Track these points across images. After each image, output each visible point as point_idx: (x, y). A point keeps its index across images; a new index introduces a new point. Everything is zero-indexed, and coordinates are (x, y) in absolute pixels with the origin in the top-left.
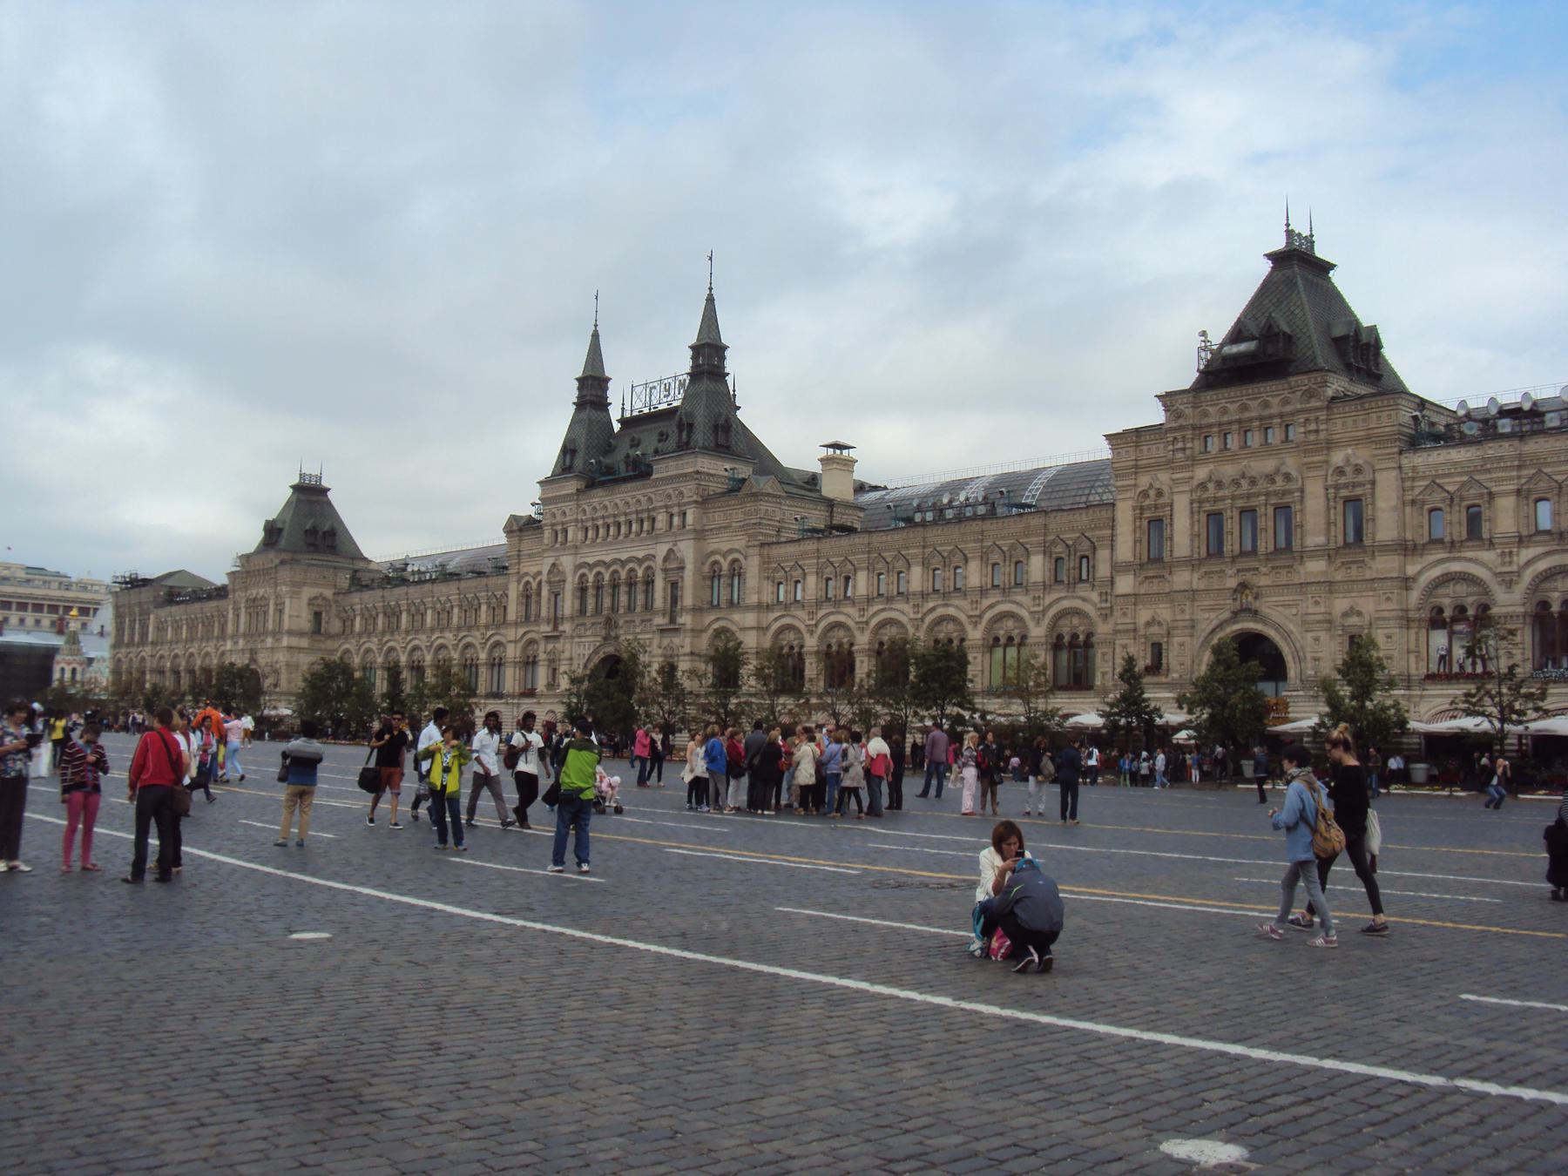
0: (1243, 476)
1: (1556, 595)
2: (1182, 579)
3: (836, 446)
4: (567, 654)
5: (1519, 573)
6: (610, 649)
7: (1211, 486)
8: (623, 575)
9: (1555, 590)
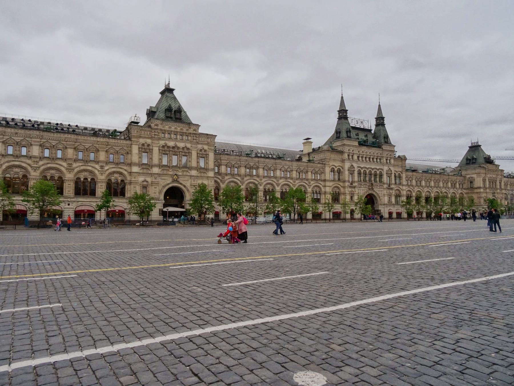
0: (166, 145)
1: (49, 174)
2: (488, 190)
3: (307, 139)
4: (357, 192)
5: (39, 168)
6: (370, 192)
7: (203, 151)
8: (373, 172)
9: (13, 171)
